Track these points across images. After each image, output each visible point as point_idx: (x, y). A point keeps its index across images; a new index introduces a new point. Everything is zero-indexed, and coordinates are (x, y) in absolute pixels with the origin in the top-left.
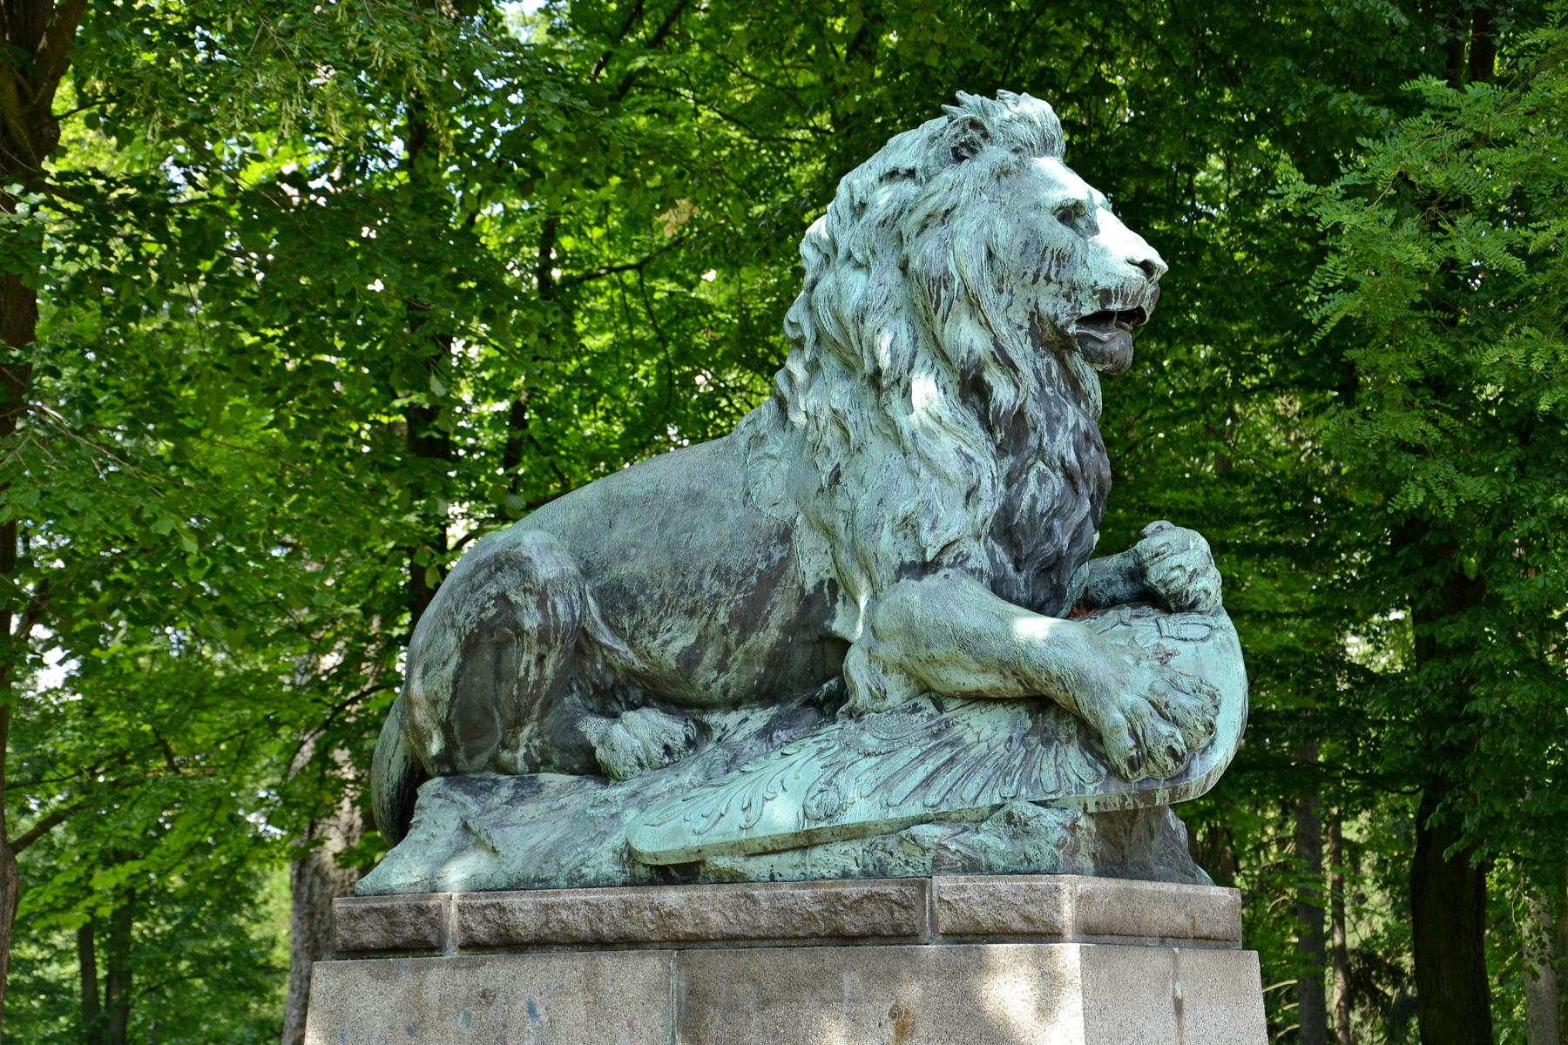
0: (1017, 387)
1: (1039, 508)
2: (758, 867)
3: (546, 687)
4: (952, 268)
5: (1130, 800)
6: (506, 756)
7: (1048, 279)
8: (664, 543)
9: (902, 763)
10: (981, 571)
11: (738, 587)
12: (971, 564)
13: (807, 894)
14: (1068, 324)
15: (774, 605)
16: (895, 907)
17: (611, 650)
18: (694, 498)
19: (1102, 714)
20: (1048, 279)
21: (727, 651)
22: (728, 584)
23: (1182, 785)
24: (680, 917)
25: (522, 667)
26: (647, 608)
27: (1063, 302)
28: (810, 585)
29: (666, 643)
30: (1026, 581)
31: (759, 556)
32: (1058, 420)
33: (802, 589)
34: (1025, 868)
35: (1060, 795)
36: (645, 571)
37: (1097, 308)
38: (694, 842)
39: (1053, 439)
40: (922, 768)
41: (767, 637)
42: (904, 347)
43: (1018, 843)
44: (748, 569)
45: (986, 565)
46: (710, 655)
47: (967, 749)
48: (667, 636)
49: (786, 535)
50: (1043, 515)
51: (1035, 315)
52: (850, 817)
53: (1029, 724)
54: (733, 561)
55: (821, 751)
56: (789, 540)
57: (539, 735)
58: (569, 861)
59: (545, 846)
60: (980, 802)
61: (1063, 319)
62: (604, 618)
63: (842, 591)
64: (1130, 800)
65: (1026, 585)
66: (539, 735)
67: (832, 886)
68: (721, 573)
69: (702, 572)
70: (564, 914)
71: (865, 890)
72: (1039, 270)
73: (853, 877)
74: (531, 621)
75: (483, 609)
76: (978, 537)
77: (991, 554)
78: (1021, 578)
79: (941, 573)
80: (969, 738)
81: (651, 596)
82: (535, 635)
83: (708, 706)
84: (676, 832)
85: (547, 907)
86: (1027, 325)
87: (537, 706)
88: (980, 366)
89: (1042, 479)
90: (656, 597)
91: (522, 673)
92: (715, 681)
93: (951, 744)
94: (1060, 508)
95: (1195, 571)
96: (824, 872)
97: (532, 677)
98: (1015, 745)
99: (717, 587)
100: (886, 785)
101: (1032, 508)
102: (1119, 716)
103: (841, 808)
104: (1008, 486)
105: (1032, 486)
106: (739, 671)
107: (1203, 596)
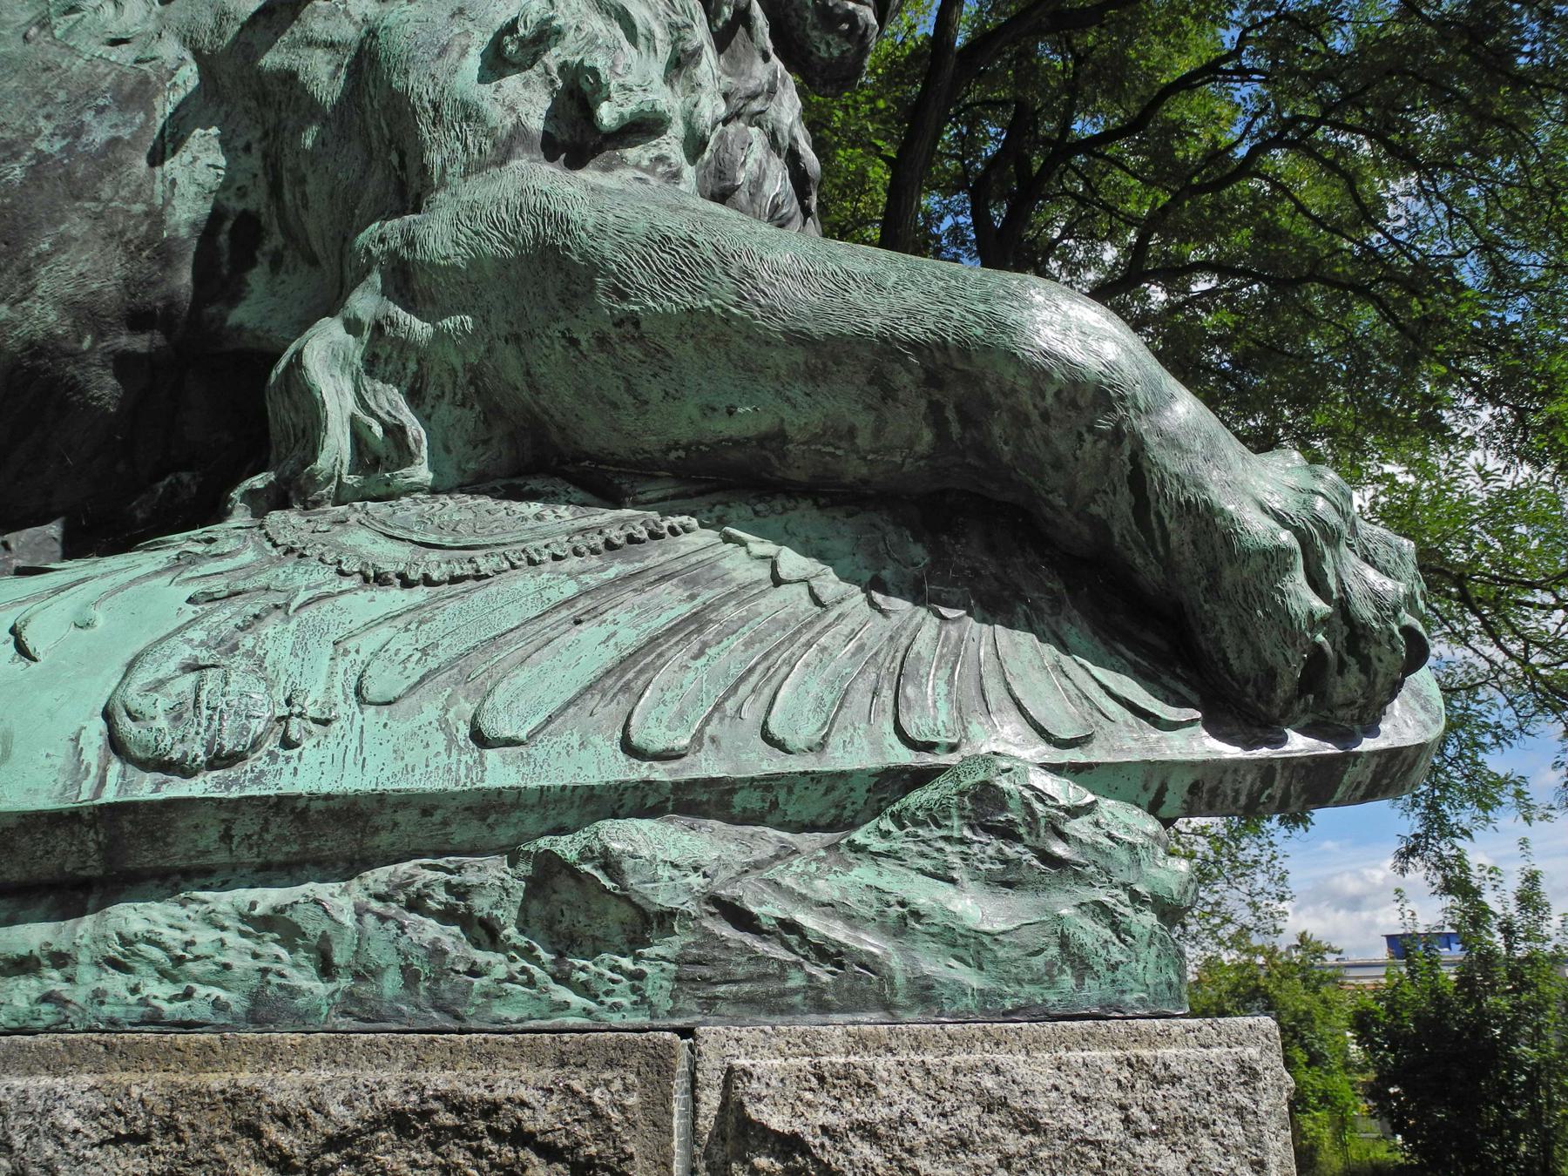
15: (62, 243)
33: (156, 217)
40: (590, 632)
53: (919, 553)
63: (275, 240)
67: (207, 1058)
71: (390, 1083)
73: (303, 1020)
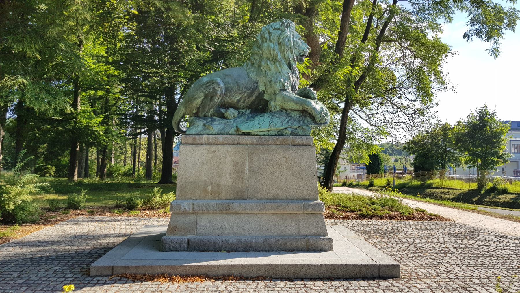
6: (207, 114)
21: (245, 100)
28: (260, 91)
41: (253, 98)
46: (242, 101)
80: (293, 116)
83: (240, 108)
100: (282, 122)
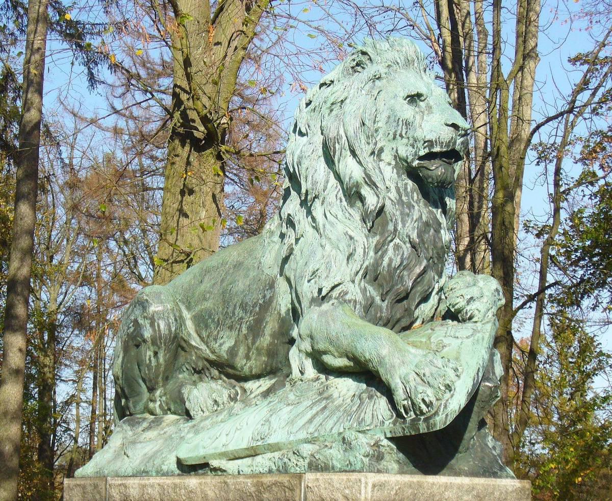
0: (378, 196)
1: (393, 265)
2: (232, 466)
3: (162, 369)
4: (342, 132)
5: (407, 430)
6: (151, 405)
7: (401, 136)
8: (221, 291)
9: (302, 409)
10: (355, 301)
11: (251, 314)
12: (348, 297)
13: (249, 481)
14: (413, 161)
15: (267, 323)
16: (287, 490)
17: (197, 348)
18: (238, 266)
19: (390, 381)
20: (401, 136)
22: (246, 313)
23: (431, 421)
24: (196, 493)
25: (147, 358)
26: (212, 326)
27: (411, 149)
29: (221, 345)
30: (387, 306)
31: (260, 296)
32: (408, 215)
34: (349, 469)
35: (372, 427)
36: (212, 306)
37: (427, 151)
38: (202, 452)
39: (404, 225)
42: (321, 177)
43: (347, 454)
44: (255, 303)
45: (359, 297)
46: (242, 351)
47: (333, 402)
48: (222, 341)
49: (272, 285)
50: (396, 269)
51: (396, 157)
52: (272, 440)
54: (249, 300)
55: (270, 402)
56: (274, 287)
57: (165, 394)
58: (157, 462)
59: (150, 453)
60: (333, 431)
61: (410, 158)
62: (197, 332)
64: (407, 430)
65: (387, 309)
66: (165, 394)
68: (243, 306)
69: (235, 306)
70: (150, 490)
72: (396, 132)
74: (147, 334)
75: (129, 328)
76: (353, 282)
77: (364, 291)
78: (384, 304)
79: (331, 302)
80: (336, 395)
81: (214, 319)
82: (149, 340)
83: (246, 379)
84: (197, 446)
85: (144, 486)
86: (393, 163)
87: (160, 379)
88: (357, 185)
89: (397, 247)
90: (216, 320)
91: (148, 362)
92: (245, 365)
93: (327, 398)
94: (408, 264)
95: (472, 298)
96: (261, 470)
97: (154, 363)
98: (356, 398)
99: (241, 314)
101: (389, 265)
102: (398, 381)
103: (270, 434)
104: (376, 253)
105: (390, 253)
106: (255, 359)
107: (476, 312)
